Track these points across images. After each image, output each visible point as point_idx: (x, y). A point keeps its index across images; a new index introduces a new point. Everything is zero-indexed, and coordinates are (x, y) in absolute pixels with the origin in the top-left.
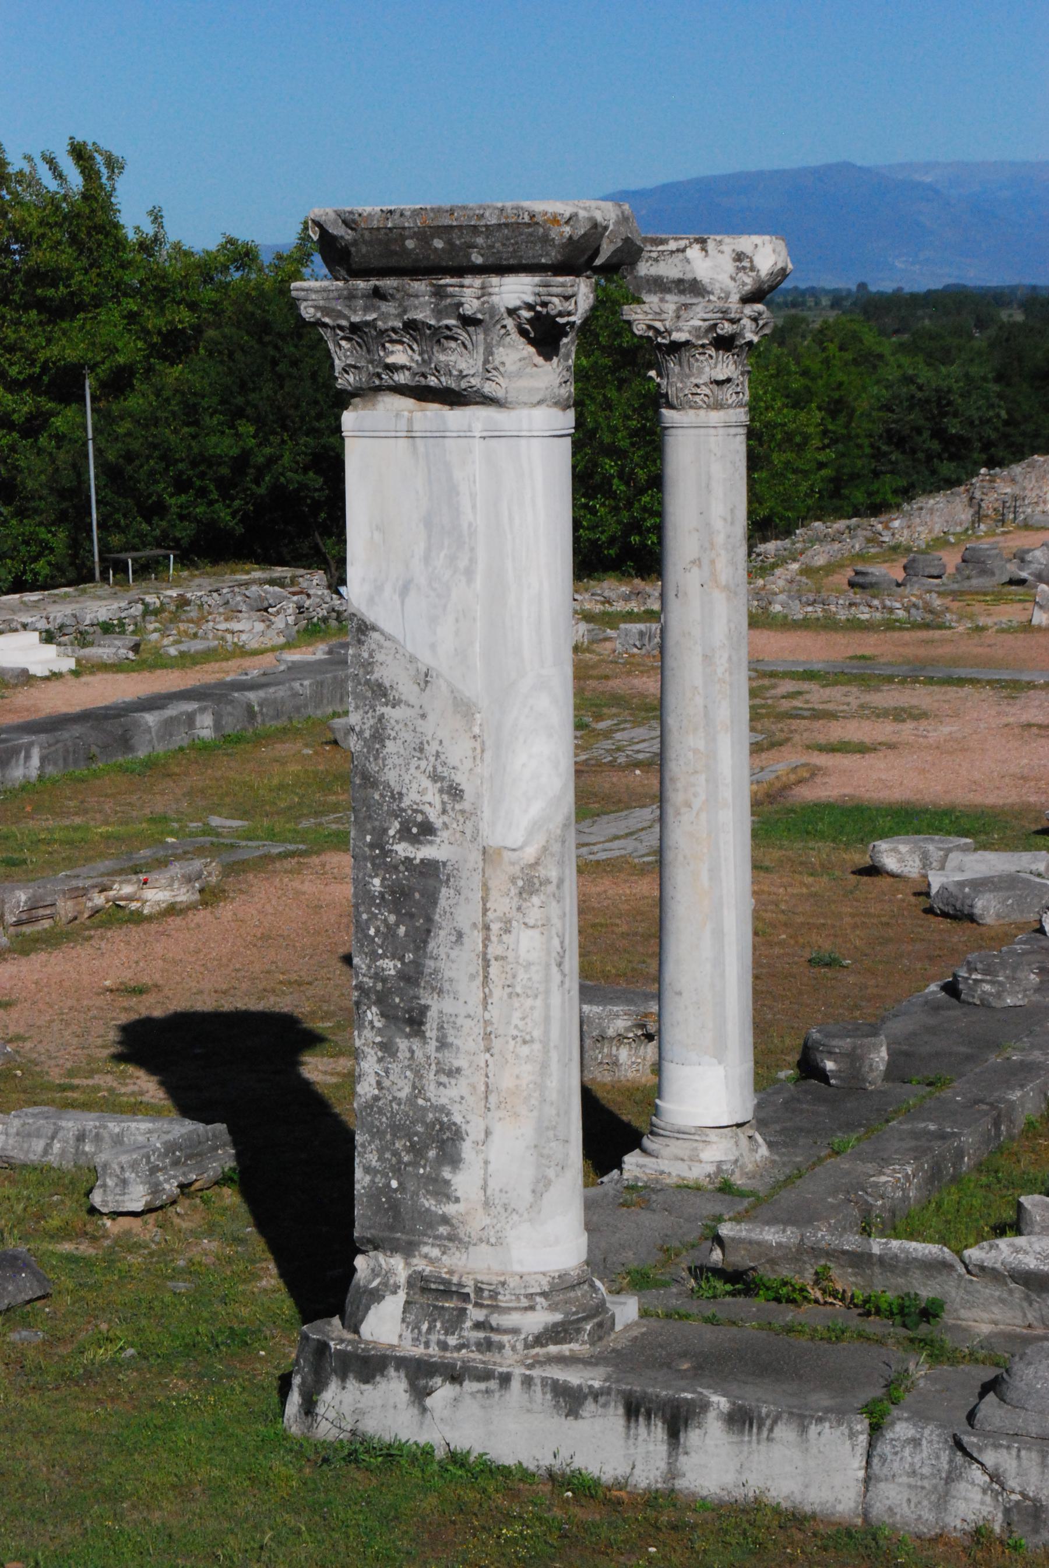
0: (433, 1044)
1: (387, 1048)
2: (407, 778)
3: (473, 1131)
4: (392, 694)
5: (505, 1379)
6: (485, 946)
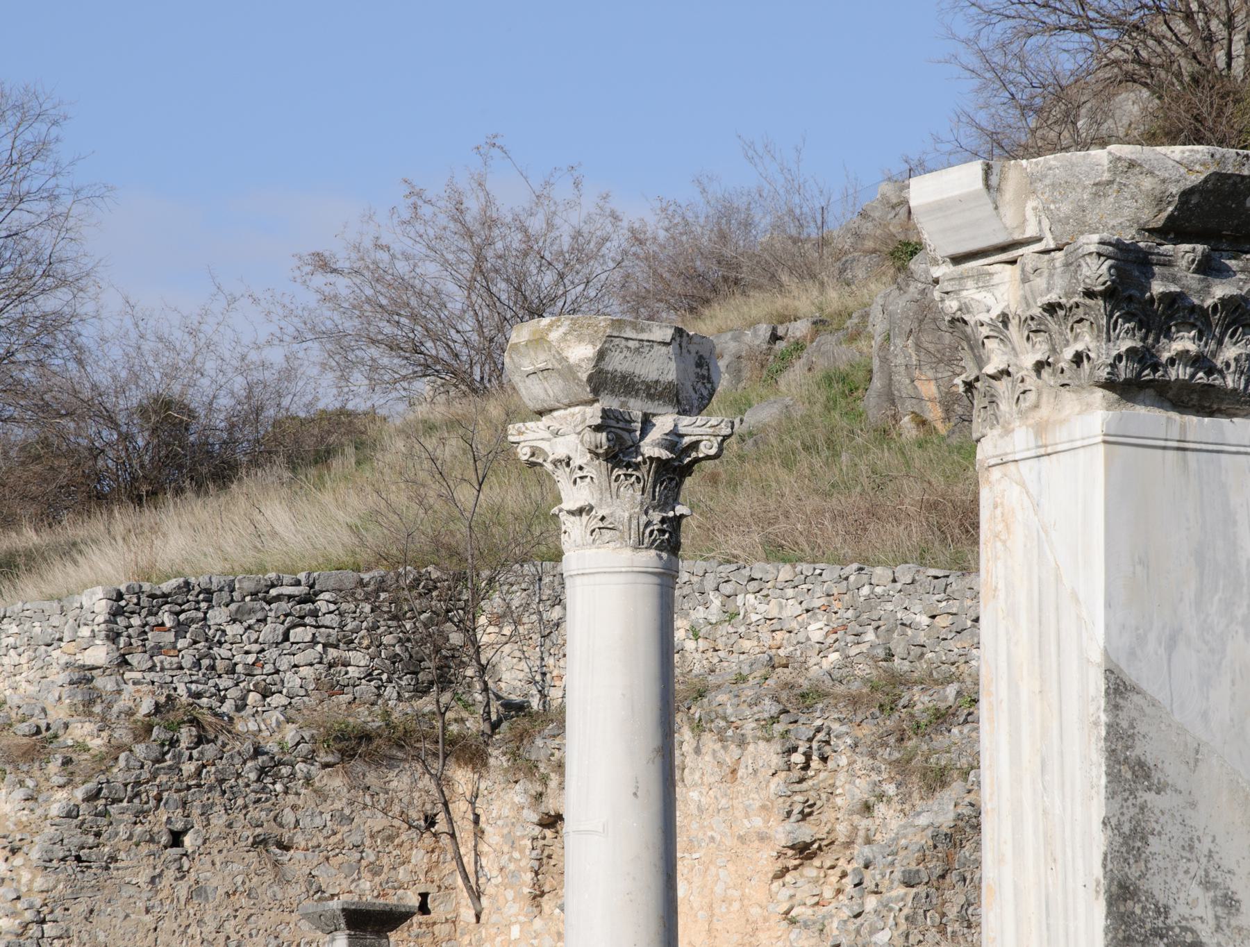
2: (1174, 885)
4: (1156, 776)
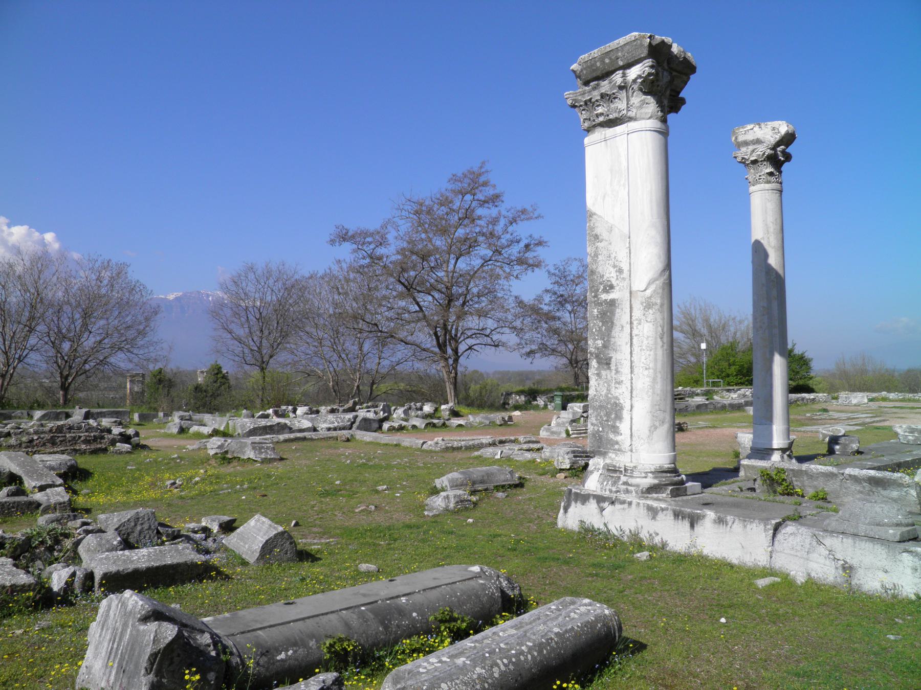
0: (614, 372)
1: (598, 375)
3: (627, 406)
4: (600, 238)
5: (630, 503)
6: (631, 331)
